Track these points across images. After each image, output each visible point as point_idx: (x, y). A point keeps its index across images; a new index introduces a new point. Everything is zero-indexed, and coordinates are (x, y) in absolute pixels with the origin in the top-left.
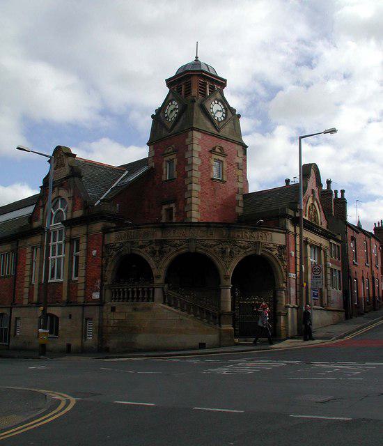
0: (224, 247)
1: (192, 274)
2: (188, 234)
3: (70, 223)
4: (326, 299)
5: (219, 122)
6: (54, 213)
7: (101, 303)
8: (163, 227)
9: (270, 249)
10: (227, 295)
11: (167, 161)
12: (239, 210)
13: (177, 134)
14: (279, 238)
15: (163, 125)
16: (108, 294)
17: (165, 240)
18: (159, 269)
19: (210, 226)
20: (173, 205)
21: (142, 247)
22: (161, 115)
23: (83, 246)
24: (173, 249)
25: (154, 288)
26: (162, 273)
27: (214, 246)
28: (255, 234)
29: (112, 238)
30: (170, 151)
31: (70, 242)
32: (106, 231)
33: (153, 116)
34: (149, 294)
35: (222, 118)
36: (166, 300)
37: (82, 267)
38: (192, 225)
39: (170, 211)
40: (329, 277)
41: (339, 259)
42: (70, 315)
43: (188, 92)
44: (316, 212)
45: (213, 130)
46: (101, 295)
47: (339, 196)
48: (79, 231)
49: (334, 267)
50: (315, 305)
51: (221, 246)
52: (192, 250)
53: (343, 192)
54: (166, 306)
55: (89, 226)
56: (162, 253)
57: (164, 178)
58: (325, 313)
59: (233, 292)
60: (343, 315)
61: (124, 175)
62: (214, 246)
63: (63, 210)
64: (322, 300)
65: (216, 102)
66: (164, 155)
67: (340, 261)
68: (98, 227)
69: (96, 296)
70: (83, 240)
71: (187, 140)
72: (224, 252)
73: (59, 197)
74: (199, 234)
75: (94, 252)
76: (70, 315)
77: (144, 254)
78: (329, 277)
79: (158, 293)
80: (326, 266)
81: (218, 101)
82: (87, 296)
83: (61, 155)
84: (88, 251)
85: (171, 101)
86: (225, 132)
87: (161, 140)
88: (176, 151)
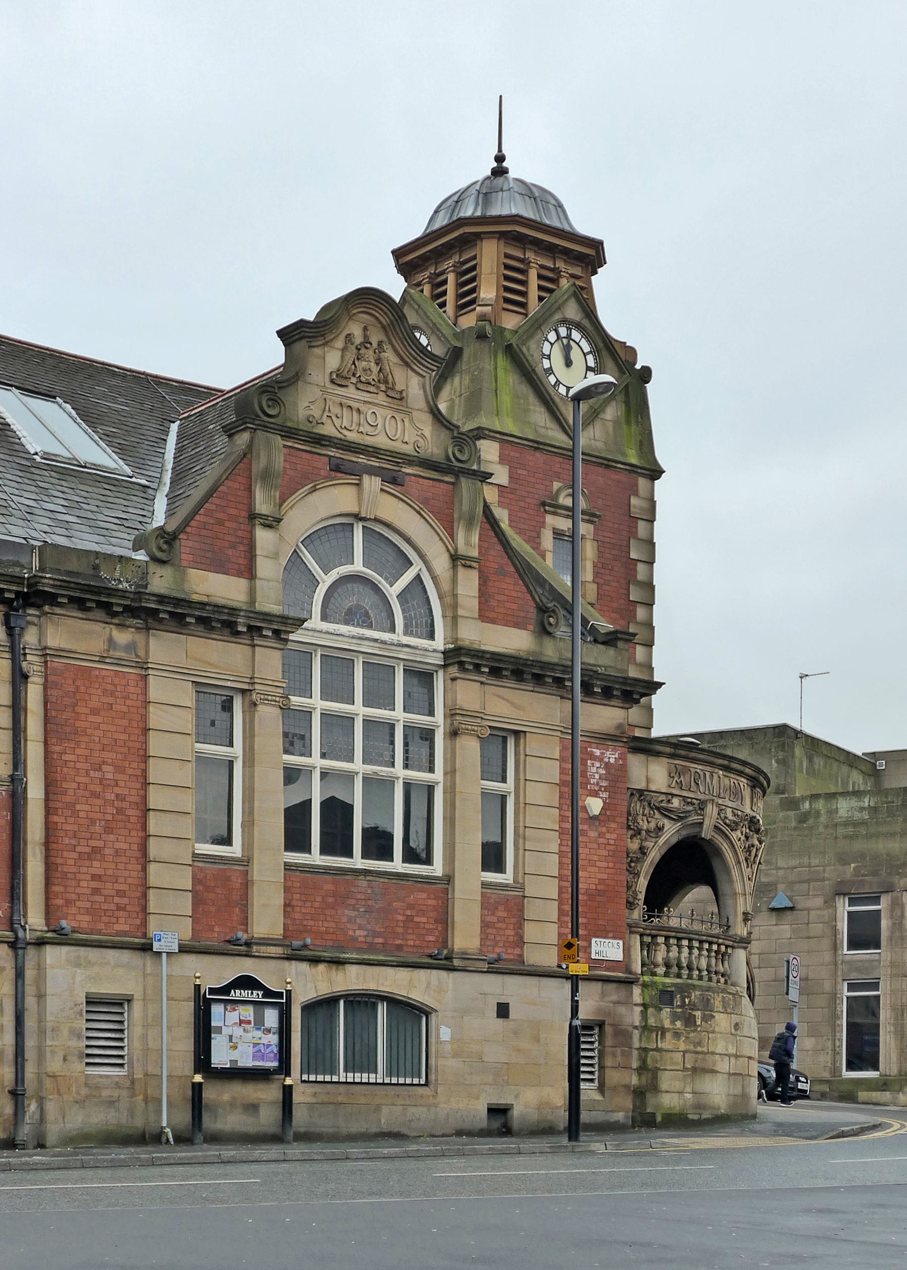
43: (467, 300)
45: (558, 437)
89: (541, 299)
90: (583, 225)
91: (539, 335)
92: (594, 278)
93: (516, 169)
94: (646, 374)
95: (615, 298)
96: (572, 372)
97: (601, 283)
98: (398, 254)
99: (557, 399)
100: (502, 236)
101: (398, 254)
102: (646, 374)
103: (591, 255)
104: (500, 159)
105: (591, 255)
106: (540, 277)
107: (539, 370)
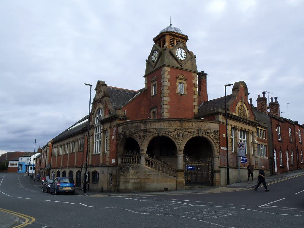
0: (179, 132)
1: (162, 147)
3: (103, 122)
5: (181, 61)
6: (98, 117)
9: (207, 133)
10: (181, 160)
11: (153, 85)
13: (157, 69)
14: (214, 126)
15: (151, 65)
17: (145, 129)
20: (155, 110)
21: (134, 134)
22: (150, 59)
24: (150, 134)
25: (140, 157)
28: (198, 124)
29: (120, 129)
30: (154, 79)
31: (103, 132)
32: (118, 125)
33: (147, 61)
34: (138, 160)
35: (184, 58)
36: (149, 163)
39: (154, 112)
40: (256, 149)
41: (266, 139)
42: (103, 172)
43: (164, 44)
44: (244, 110)
45: (178, 66)
46: (116, 161)
47: (274, 101)
48: (107, 126)
49: (261, 143)
51: (176, 132)
52: (161, 135)
53: (276, 98)
55: (112, 123)
56: (144, 137)
57: (152, 95)
63: (101, 115)
66: (152, 82)
67: (266, 140)
68: (115, 123)
69: (114, 161)
70: (109, 131)
71: (162, 72)
72: (178, 135)
73: (100, 108)
76: (103, 172)
78: (256, 149)
79: (143, 159)
80: (253, 142)
81: (181, 48)
83: (101, 85)
85: (155, 51)
88: (156, 79)
89: (176, 44)
90: (184, 33)
91: (175, 49)
93: (173, 25)
95: (189, 45)
96: (180, 54)
97: (188, 43)
98: (154, 39)
101: (154, 39)
102: (195, 57)
103: (186, 38)
104: (171, 24)
105: (186, 38)
106: (176, 41)
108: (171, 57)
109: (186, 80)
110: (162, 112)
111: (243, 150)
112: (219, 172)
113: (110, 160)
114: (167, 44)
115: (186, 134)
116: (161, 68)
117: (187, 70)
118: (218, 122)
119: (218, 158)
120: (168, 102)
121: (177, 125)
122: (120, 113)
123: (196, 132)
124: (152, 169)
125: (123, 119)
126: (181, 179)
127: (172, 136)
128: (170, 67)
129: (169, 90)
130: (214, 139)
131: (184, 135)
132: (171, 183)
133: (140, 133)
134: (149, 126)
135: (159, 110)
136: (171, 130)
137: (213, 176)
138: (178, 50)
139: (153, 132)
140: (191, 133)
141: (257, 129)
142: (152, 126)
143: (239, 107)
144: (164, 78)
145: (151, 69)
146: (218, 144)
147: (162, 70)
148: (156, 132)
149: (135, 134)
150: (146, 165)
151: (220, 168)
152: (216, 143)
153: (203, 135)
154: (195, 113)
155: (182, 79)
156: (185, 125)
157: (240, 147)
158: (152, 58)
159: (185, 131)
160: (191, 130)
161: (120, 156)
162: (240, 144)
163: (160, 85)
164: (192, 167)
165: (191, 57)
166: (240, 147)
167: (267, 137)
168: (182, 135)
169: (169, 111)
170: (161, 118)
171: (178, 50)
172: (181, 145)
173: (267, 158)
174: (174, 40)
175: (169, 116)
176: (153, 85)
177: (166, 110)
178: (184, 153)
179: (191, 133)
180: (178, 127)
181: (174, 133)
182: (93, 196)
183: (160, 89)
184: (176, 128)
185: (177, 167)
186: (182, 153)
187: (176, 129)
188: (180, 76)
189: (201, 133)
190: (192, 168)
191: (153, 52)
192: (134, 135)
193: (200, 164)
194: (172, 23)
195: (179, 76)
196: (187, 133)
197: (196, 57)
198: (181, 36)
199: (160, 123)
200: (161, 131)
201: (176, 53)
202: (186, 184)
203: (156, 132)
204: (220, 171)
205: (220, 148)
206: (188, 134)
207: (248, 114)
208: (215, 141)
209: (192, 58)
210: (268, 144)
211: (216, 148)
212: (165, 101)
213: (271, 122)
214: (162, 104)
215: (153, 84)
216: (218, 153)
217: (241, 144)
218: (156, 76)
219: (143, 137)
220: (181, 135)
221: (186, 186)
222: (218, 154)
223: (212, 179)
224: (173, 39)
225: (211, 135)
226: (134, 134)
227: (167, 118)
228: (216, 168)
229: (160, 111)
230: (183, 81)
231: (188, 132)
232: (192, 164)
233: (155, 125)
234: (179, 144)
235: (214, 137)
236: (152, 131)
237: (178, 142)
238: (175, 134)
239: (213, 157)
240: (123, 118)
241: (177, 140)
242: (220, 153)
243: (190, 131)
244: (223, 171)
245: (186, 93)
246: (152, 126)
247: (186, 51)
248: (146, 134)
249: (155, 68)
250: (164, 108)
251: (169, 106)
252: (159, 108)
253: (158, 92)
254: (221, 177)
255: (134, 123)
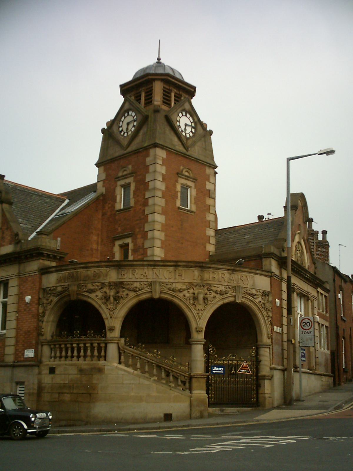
0: (196, 292)
1: (156, 324)
2: (150, 274)
4: (314, 360)
5: (188, 139)
7: (37, 362)
8: (119, 266)
9: (252, 295)
10: (198, 352)
11: (122, 186)
12: (211, 248)
13: (136, 152)
14: (263, 283)
15: (118, 142)
16: (46, 350)
17: (122, 283)
18: (115, 319)
19: (179, 266)
20: (129, 241)
22: (115, 128)
23: (13, 290)
24: (132, 294)
25: (106, 344)
26: (118, 324)
27: (184, 290)
28: (237, 276)
29: (51, 280)
30: (125, 173)
32: (45, 271)
33: (103, 131)
34: (99, 352)
35: (191, 134)
37: (12, 316)
38: (155, 264)
41: (327, 312)
43: (149, 100)
44: (302, 253)
45: (181, 149)
46: (36, 353)
47: (320, 238)
49: (322, 322)
50: (302, 368)
51: (191, 291)
52: (157, 296)
53: (324, 233)
54: (122, 366)
56: (117, 299)
58: (313, 377)
59: (206, 350)
60: (331, 380)
61: (64, 204)
62: (184, 290)
64: (309, 363)
65: (184, 113)
66: (118, 178)
67: (328, 315)
68: (34, 266)
70: (13, 283)
71: (148, 159)
72: (195, 298)
74: (165, 275)
75: (28, 298)
77: (95, 299)
79: (112, 350)
82: (19, 353)
84: (21, 297)
85: (127, 111)
86: (196, 152)
87: (113, 160)
89: (175, 103)
91: (176, 114)
92: (192, 100)
94: (211, 133)
98: (122, 86)
99: (182, 137)
100: (162, 80)
101: (122, 86)
102: (211, 133)
103: (190, 91)
104: (159, 59)
105: (190, 91)
106: (175, 96)
107: (176, 125)
108: (168, 129)
109: (194, 180)
110: (147, 244)
111: (310, 333)
112: (271, 378)
113: (16, 350)
114: (158, 99)
115: (212, 296)
116: (145, 150)
117: (197, 160)
118: (270, 274)
119: (268, 350)
120: (162, 224)
121: (192, 275)
122: (48, 244)
123: (231, 293)
124: (135, 372)
125: (54, 258)
126: (200, 393)
127: (182, 300)
128: (166, 150)
129: (163, 200)
130: (263, 309)
131: (207, 299)
132: (177, 403)
133: (106, 289)
134: (131, 274)
135: (139, 241)
136: (179, 288)
137: (258, 386)
138: (180, 115)
139: (139, 290)
140: (221, 294)
141: (318, 292)
142: (137, 276)
143: (296, 246)
144: (155, 171)
145: (117, 152)
146: (270, 319)
147: (148, 155)
148: (146, 290)
149: (95, 292)
150: (120, 363)
151: (272, 371)
152: (266, 318)
153: (244, 300)
154: (211, 254)
155: (187, 178)
156: (208, 275)
157: (304, 327)
158: (120, 127)
159: (209, 290)
160: (221, 288)
161: (49, 343)
162: (303, 321)
163: (143, 186)
164: (220, 369)
165: (203, 133)
166: (304, 327)
167: (328, 311)
168: (204, 299)
169: (164, 245)
170: (145, 259)
171: (180, 115)
172: (199, 319)
173: (329, 352)
174: (170, 93)
175: (163, 255)
176: (122, 186)
177: (158, 243)
178: (205, 338)
179: (221, 294)
180: (195, 281)
181: (185, 292)
182: (111, 428)
183: (144, 195)
184: (190, 283)
185: (190, 368)
186: (201, 336)
187: (191, 285)
188: (184, 171)
189: (241, 295)
190: (220, 370)
191: (122, 112)
192: (93, 295)
193: (235, 362)
194: (161, 57)
195: (182, 171)
196: (213, 294)
197: (211, 135)
198: (180, 84)
199: (155, 271)
200: (158, 288)
201: (177, 121)
202: (210, 405)
203: (146, 289)
204: (272, 377)
205: (272, 329)
206: (214, 297)
207: (306, 261)
208: (264, 313)
209: (204, 136)
210: (330, 323)
211: (265, 328)
212: (156, 223)
213: (334, 280)
214: (147, 228)
215: (122, 182)
216: (269, 338)
217: (306, 321)
218: (130, 167)
219: (115, 299)
220: (201, 297)
221: (211, 410)
222: (269, 341)
223: (257, 393)
224: (169, 90)
225: (257, 301)
226: (90, 293)
227: (159, 259)
228: (265, 371)
229: (143, 244)
230: (190, 183)
231: (216, 292)
232: (221, 362)
233: (144, 274)
234: (197, 317)
235: (263, 305)
236: (136, 287)
237: (195, 312)
238: (187, 295)
239: (257, 349)
240: (53, 255)
241: (192, 307)
242: (272, 339)
243: (219, 289)
244: (278, 376)
245: (194, 209)
246: (137, 276)
247: (196, 120)
248: (123, 293)
249: (130, 149)
250: (153, 238)
251: (163, 234)
252: (139, 236)
253: (136, 203)
254: (272, 389)
255: (90, 267)
